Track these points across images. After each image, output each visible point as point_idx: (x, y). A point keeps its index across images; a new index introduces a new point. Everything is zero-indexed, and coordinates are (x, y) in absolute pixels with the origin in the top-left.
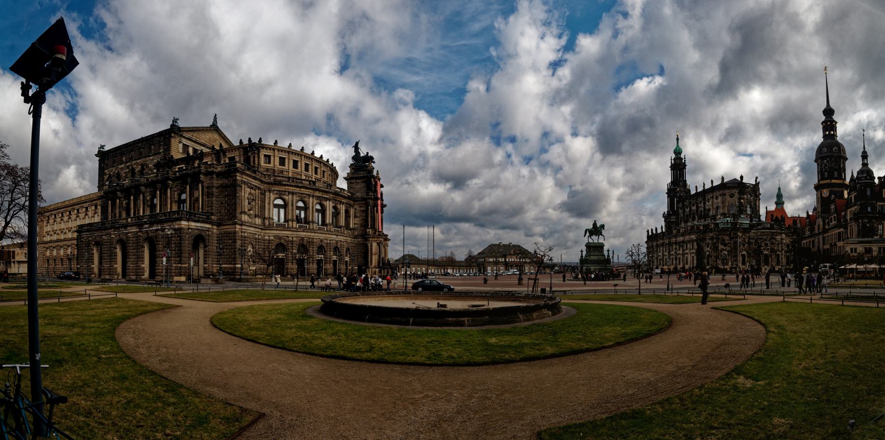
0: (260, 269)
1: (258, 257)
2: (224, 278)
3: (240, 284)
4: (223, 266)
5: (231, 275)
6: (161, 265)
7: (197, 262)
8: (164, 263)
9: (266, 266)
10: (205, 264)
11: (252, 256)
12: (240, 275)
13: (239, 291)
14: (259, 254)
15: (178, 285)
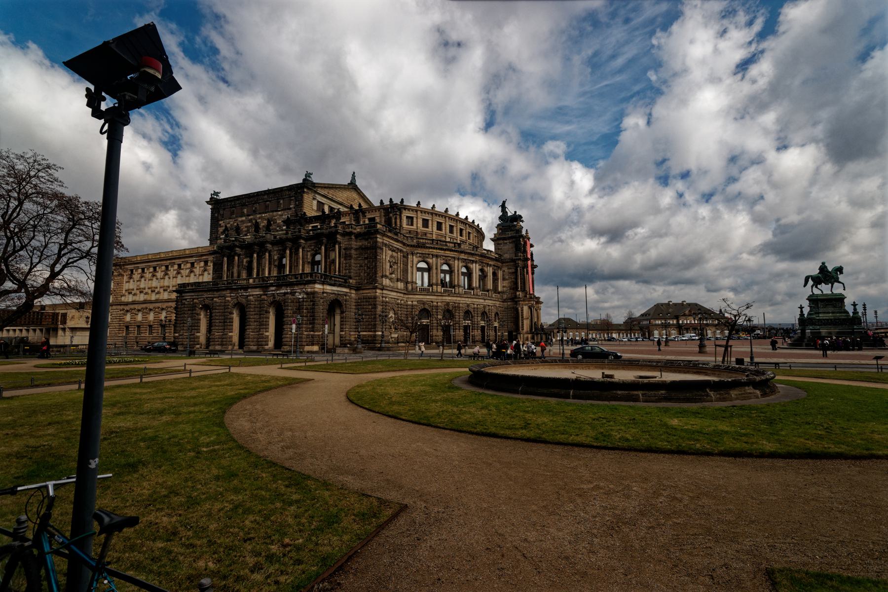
0: (403, 336)
1: (400, 324)
2: (363, 347)
3: (381, 353)
4: (361, 333)
5: (371, 344)
6: (290, 333)
7: (332, 329)
8: (294, 331)
9: (409, 333)
10: (341, 331)
11: (393, 323)
12: (381, 343)
13: (379, 361)
14: (402, 320)
15: (309, 355)
